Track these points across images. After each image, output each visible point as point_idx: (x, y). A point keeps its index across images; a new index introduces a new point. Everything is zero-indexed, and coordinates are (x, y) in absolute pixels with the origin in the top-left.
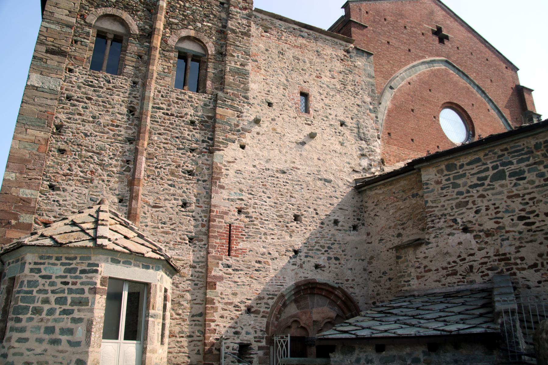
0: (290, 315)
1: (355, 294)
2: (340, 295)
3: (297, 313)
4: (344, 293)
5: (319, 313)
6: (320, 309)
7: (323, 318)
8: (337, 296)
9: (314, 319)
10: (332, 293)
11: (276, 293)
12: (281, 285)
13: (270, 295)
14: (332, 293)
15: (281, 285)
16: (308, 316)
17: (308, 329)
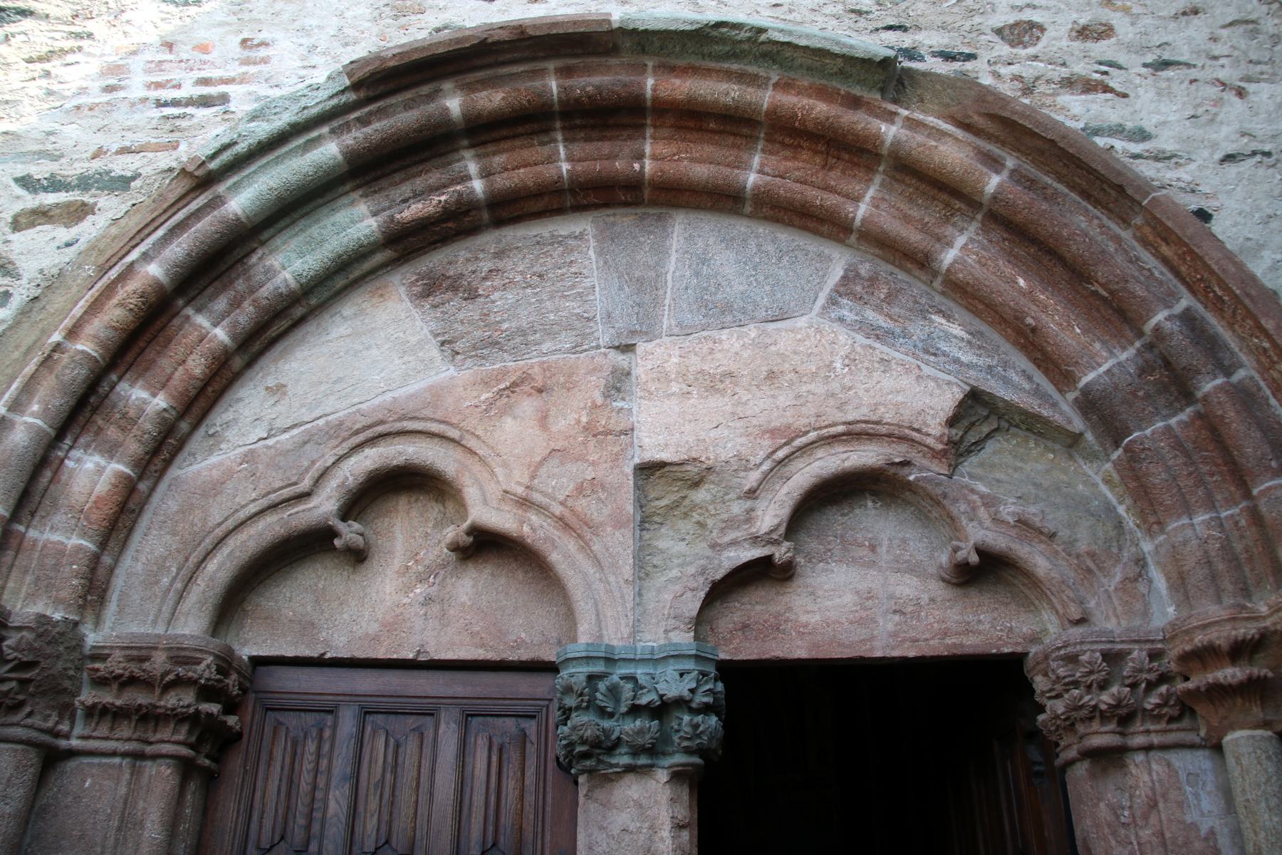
0: (338, 407)
1: (1141, 135)
2: (952, 152)
3: (436, 394)
4: (1006, 127)
5: (715, 383)
6: (730, 341)
7: (786, 434)
8: (911, 173)
9: (654, 443)
10: (853, 152)
11: (122, 166)
12: (205, 102)
13: (55, 184)
14: (853, 152)
15: (205, 102)
16: (569, 416)
17: (563, 554)
